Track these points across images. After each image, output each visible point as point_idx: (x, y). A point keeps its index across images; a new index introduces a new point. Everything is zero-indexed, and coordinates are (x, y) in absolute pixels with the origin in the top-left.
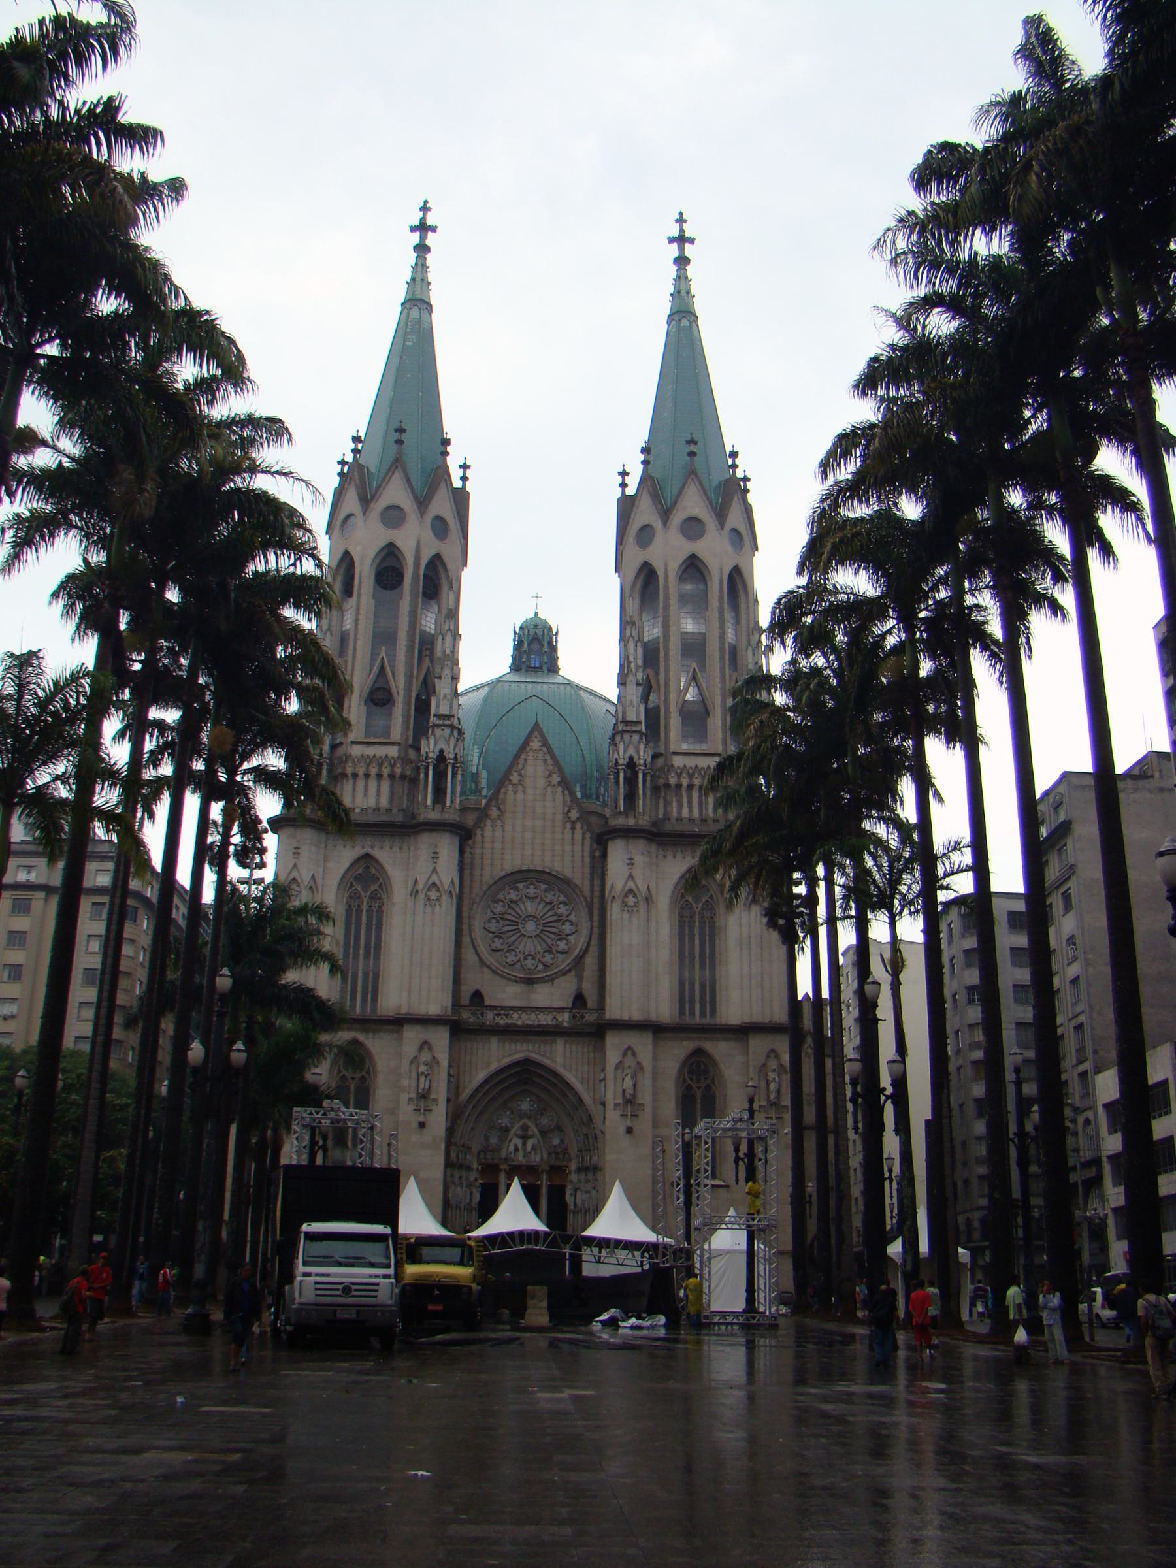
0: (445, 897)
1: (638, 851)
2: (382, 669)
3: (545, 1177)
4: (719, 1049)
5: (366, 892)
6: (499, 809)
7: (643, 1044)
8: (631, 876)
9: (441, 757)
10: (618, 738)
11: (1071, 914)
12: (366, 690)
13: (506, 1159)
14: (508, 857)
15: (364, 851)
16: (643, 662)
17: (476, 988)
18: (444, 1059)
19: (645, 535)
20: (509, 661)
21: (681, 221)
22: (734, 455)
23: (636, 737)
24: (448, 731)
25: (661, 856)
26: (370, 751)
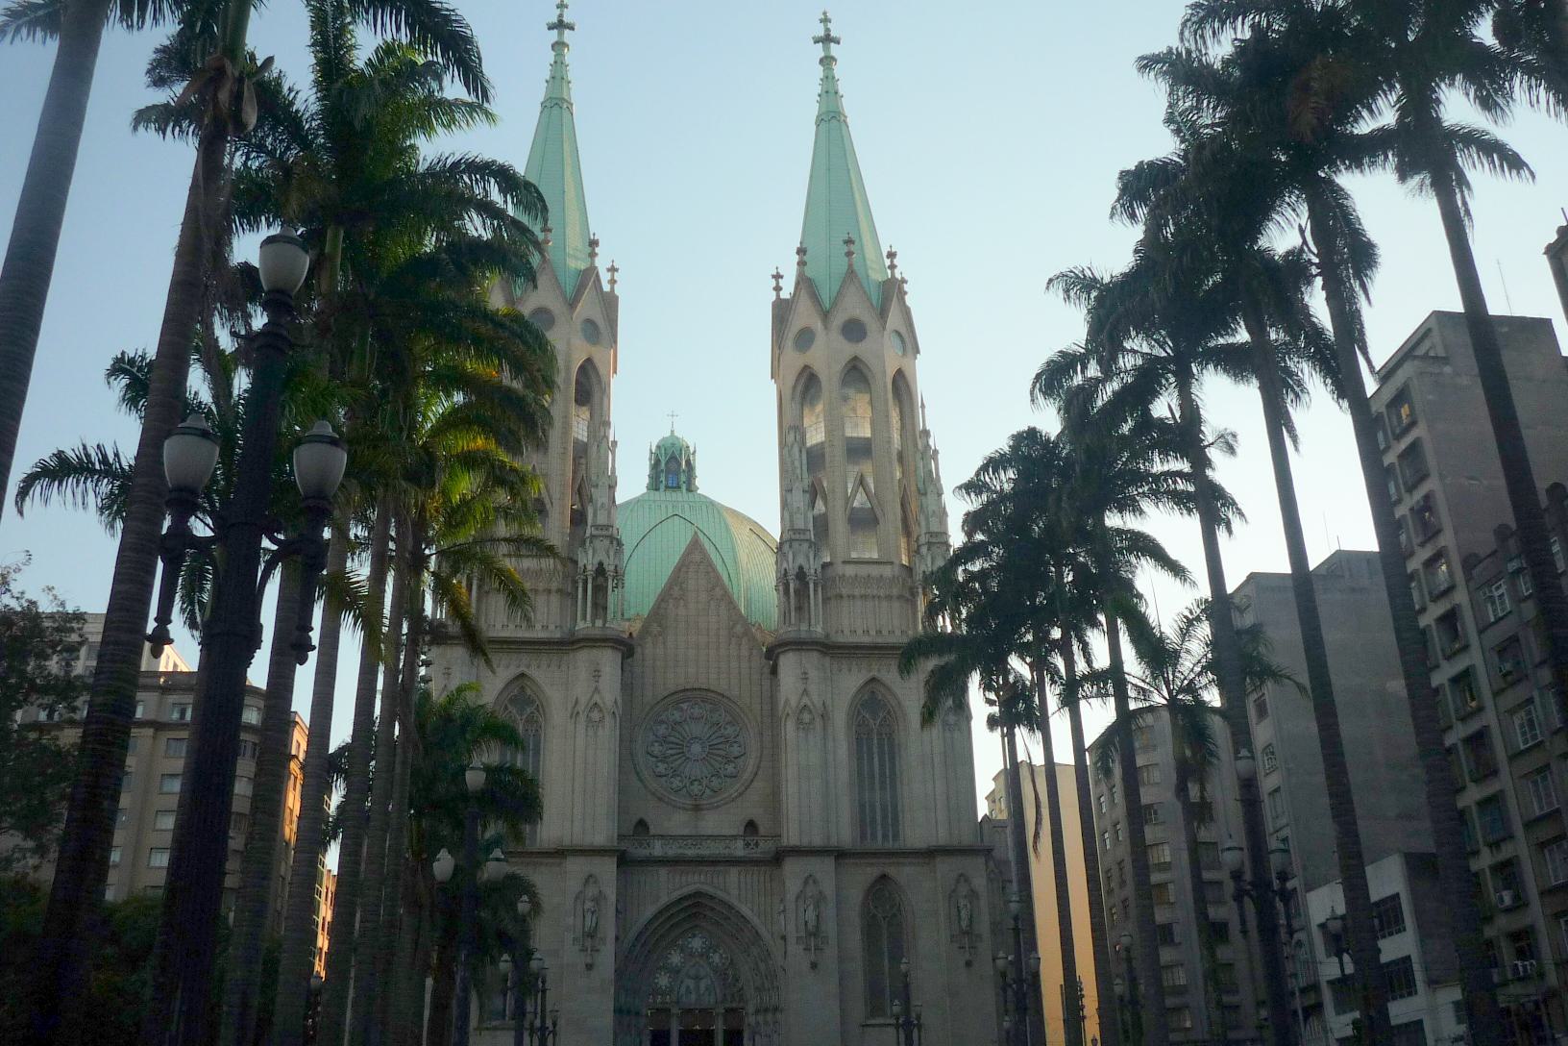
0: (608, 719)
1: (812, 659)
4: (905, 874)
7: (824, 870)
8: (805, 692)
9: (600, 570)
10: (786, 547)
11: (1267, 722)
16: (804, 470)
19: (805, 339)
20: (646, 480)
21: (825, 20)
22: (891, 255)
23: (806, 545)
24: (607, 542)
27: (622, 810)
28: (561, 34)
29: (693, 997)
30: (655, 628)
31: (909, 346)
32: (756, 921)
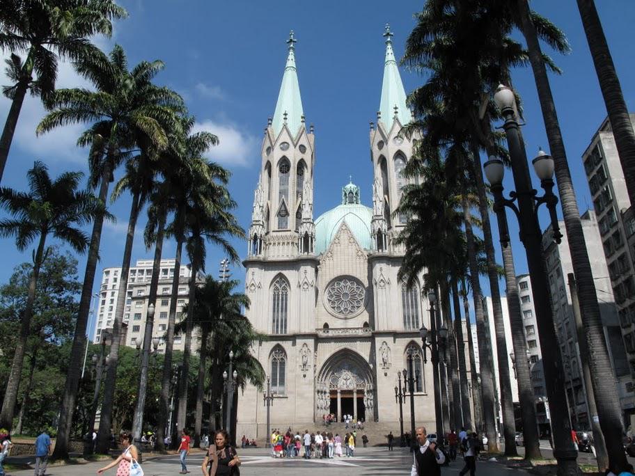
2: (283, 203)
7: (390, 340)
9: (306, 234)
14: (335, 271)
26: (280, 234)
27: (317, 319)
29: (345, 386)
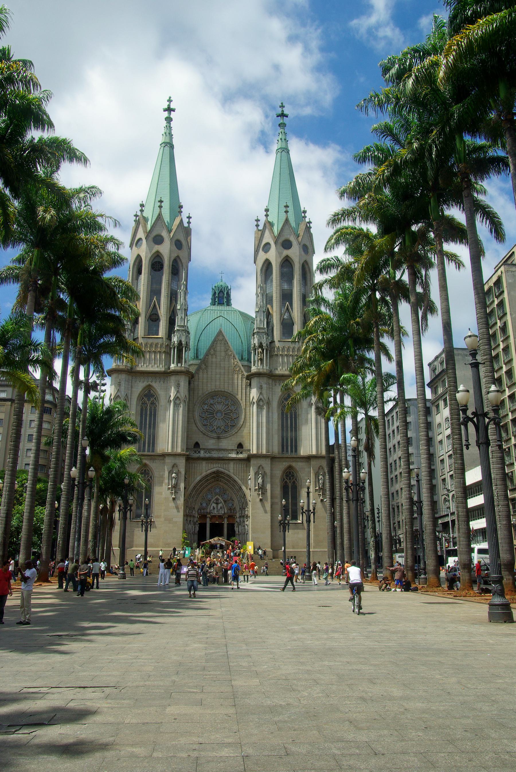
2: (155, 305)
3: (226, 520)
4: (298, 465)
5: (149, 401)
6: (205, 365)
12: (148, 315)
13: (210, 513)
14: (209, 385)
15: (147, 384)
17: (196, 441)
18: (183, 471)
20: (210, 301)
22: (305, 212)
25: (273, 385)
28: (170, 114)
30: (203, 366)
31: (310, 250)
32: (239, 482)
